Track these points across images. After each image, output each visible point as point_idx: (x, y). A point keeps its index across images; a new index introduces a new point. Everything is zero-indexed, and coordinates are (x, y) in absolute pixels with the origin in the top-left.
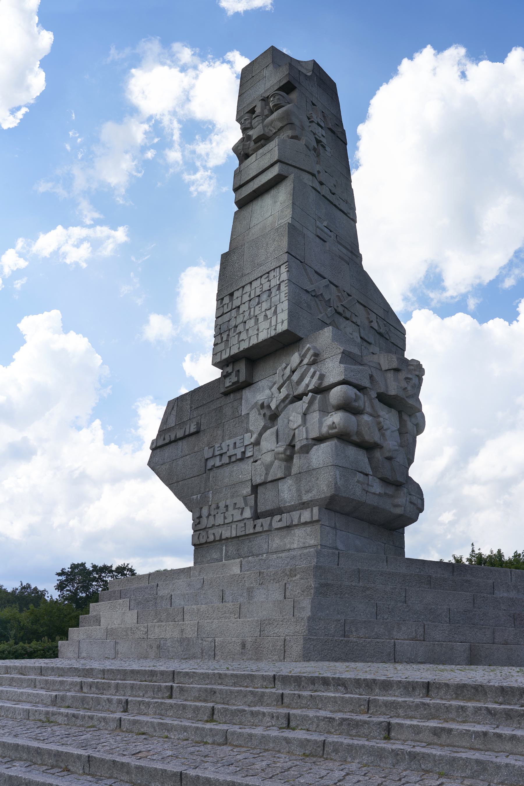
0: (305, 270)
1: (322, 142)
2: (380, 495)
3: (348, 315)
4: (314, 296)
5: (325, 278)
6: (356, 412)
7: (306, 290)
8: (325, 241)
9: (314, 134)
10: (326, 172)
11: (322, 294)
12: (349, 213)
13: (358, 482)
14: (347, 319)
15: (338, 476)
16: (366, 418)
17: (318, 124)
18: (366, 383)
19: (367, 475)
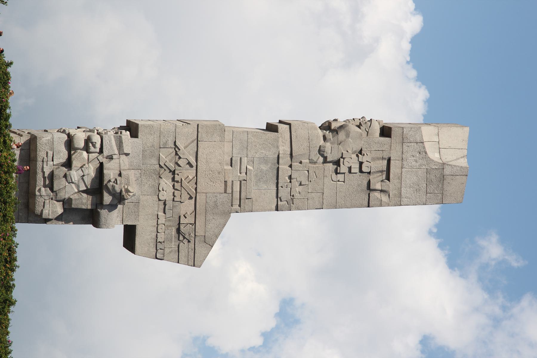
0: (193, 141)
1: (340, 167)
2: (44, 173)
3: (177, 186)
4: (176, 151)
5: (197, 163)
6: (86, 148)
7: (175, 142)
8: (231, 166)
9: (342, 157)
10: (308, 171)
11: (180, 158)
12: (281, 201)
13: (47, 153)
14: (174, 186)
15: (47, 138)
16: (85, 154)
17: (361, 164)
18: (106, 153)
19: (53, 161)
